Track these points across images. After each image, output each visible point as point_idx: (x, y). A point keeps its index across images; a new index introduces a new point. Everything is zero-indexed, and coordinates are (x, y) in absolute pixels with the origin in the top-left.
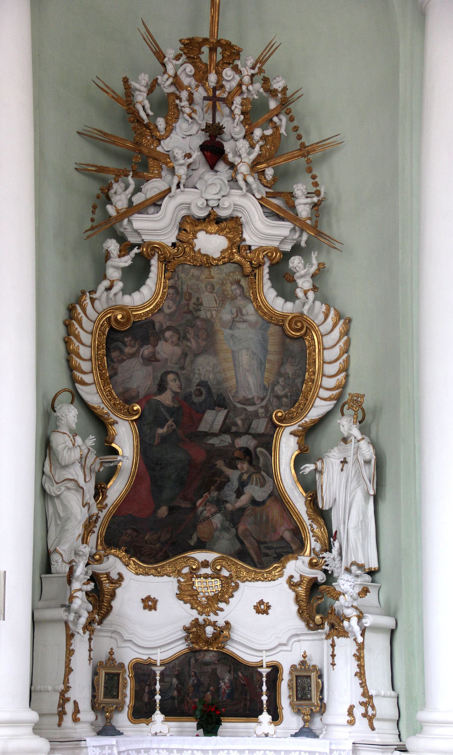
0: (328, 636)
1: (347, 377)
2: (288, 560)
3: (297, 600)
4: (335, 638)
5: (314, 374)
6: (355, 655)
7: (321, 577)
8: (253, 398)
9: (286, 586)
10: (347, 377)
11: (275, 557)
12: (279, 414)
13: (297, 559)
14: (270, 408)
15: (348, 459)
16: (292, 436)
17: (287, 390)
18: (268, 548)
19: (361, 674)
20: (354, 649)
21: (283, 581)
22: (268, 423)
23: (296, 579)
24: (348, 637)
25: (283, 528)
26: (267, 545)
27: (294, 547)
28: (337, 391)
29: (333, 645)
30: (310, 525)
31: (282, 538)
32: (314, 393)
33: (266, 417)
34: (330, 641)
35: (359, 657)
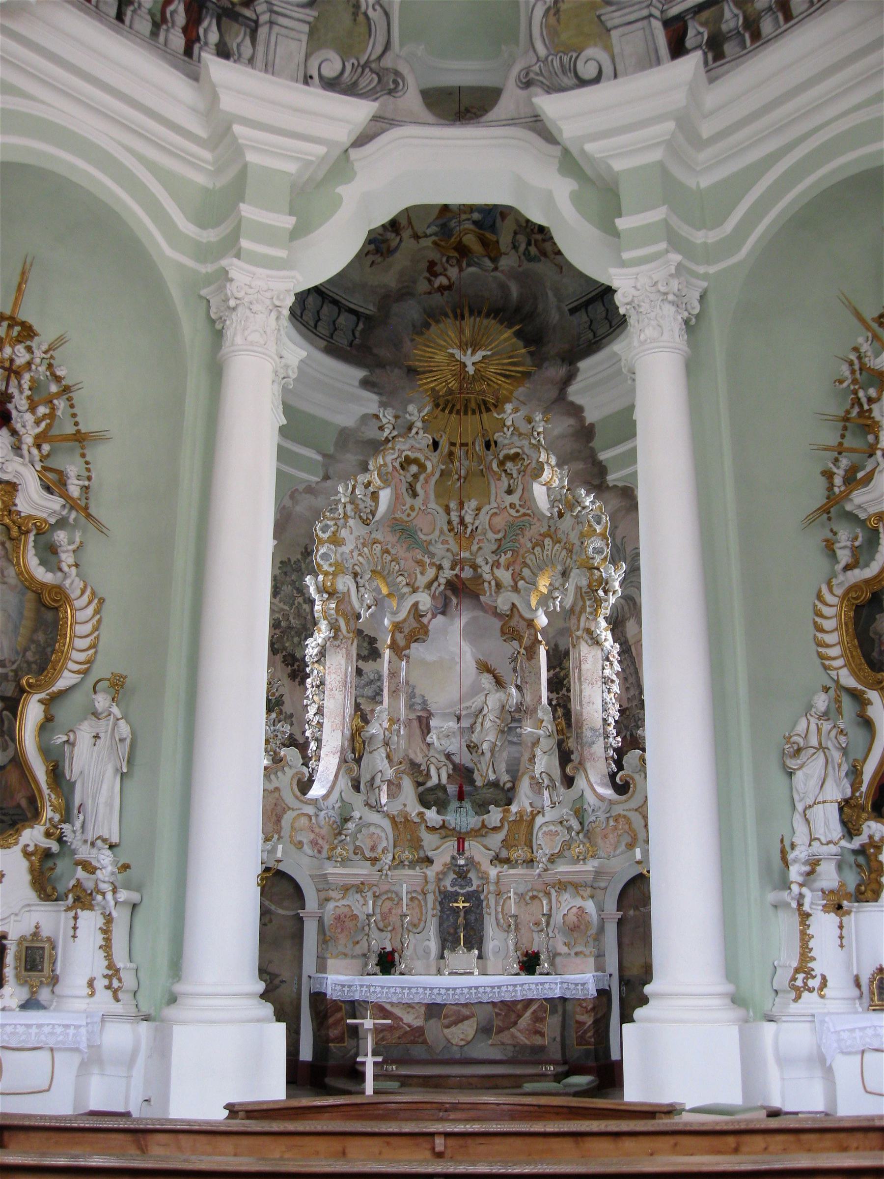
0: (69, 909)
1: (96, 653)
2: (24, 828)
3: (32, 870)
4: (79, 911)
5: (64, 645)
6: (100, 929)
7: (55, 847)
8: (5, 660)
9: (21, 854)
10: (96, 653)
11: (11, 825)
12: (31, 681)
13: (32, 827)
14: (20, 673)
15: (101, 735)
16: (39, 704)
17: (37, 657)
18: (4, 814)
19: (107, 947)
20: (101, 922)
21: (17, 849)
22: (16, 687)
23: (31, 849)
24: (93, 910)
25: (20, 795)
26: (3, 811)
27: (29, 815)
28: (86, 666)
29: (76, 918)
30: (49, 795)
31: (19, 806)
32: (63, 664)
33: (15, 681)
34: (72, 914)
35: (106, 931)
